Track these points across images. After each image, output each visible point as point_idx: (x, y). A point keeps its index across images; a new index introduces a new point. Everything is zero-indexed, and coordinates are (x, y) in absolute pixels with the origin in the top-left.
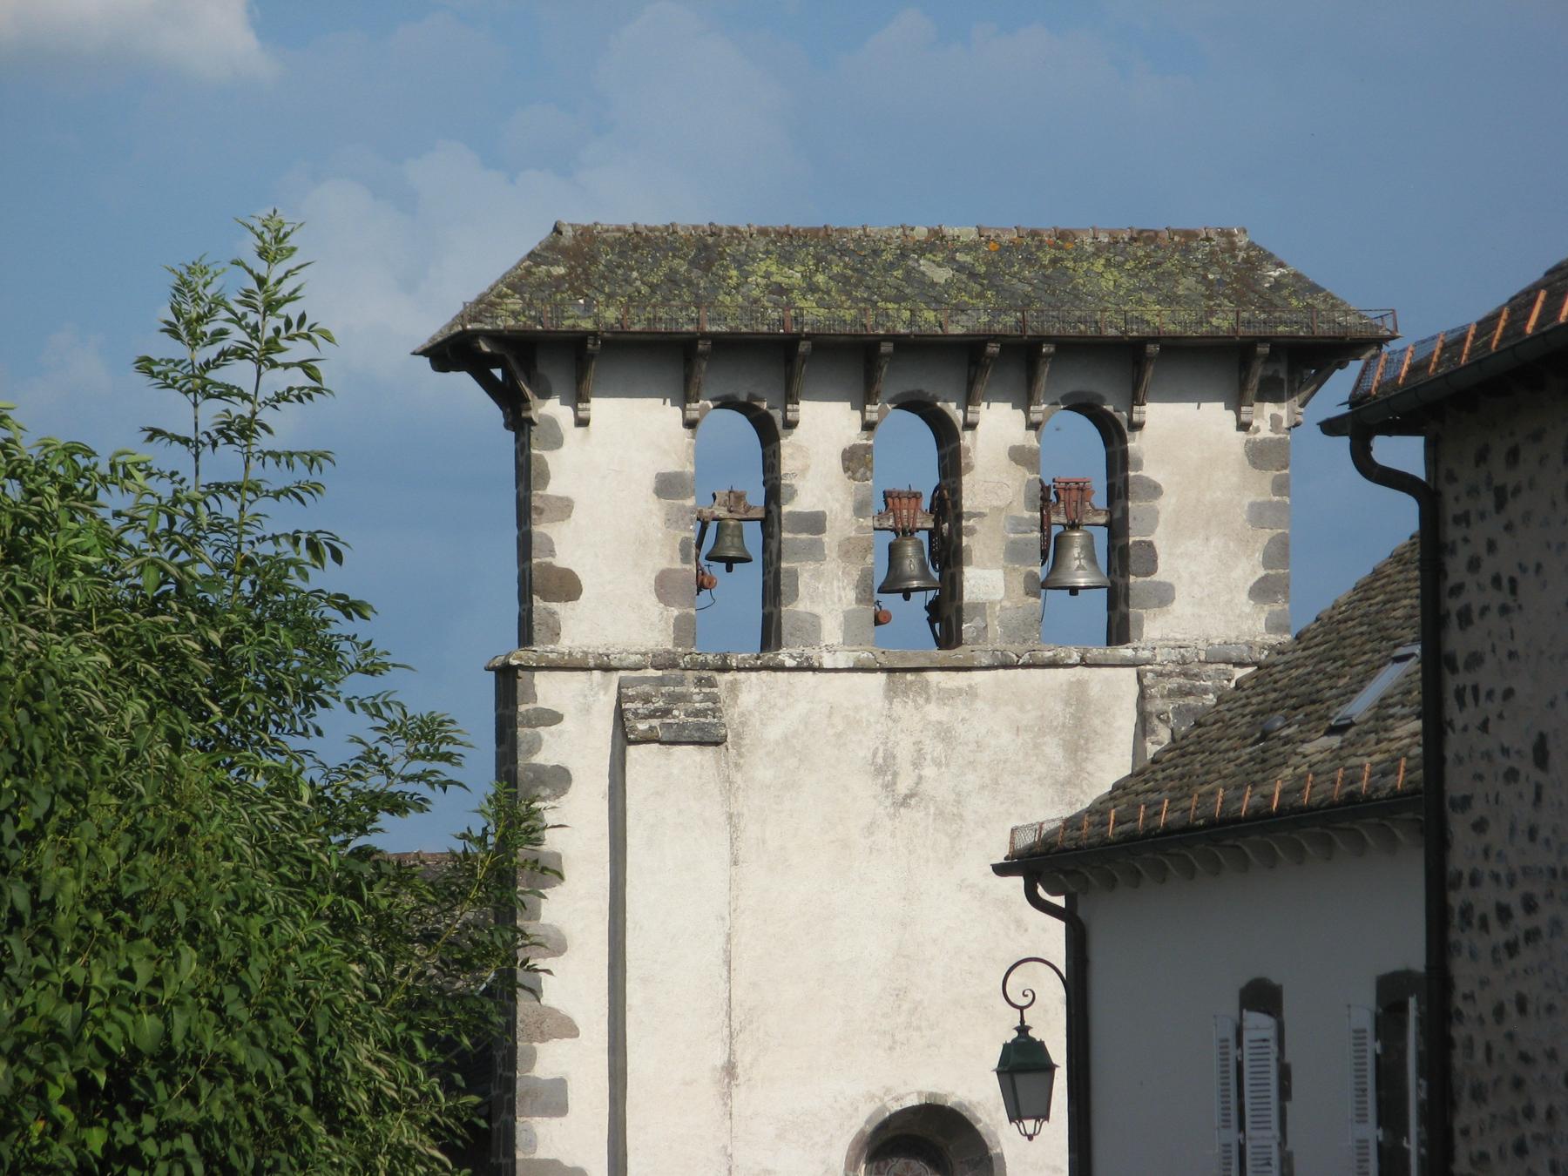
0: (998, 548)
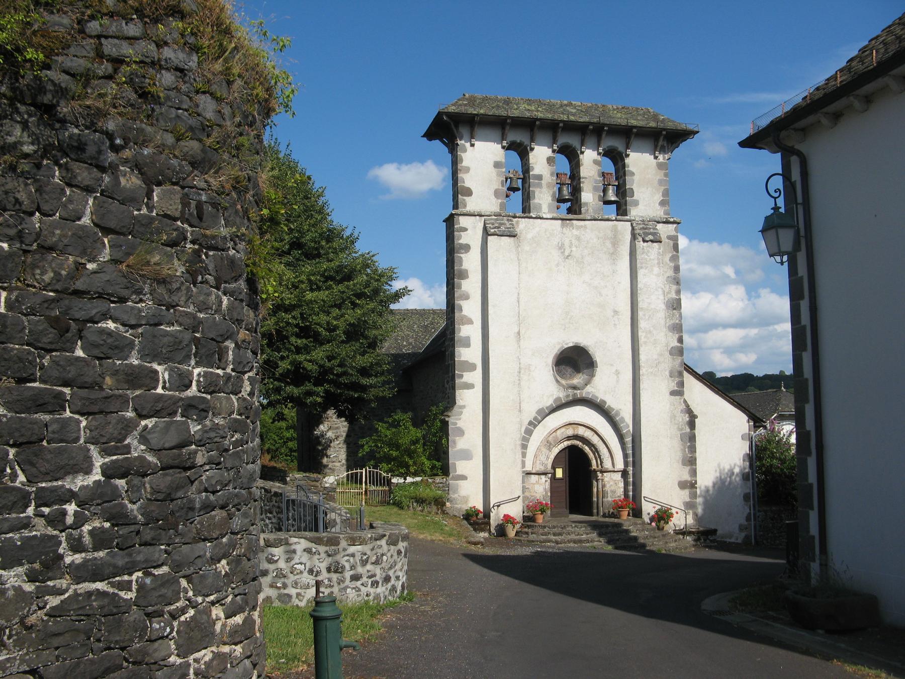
0: (591, 188)
